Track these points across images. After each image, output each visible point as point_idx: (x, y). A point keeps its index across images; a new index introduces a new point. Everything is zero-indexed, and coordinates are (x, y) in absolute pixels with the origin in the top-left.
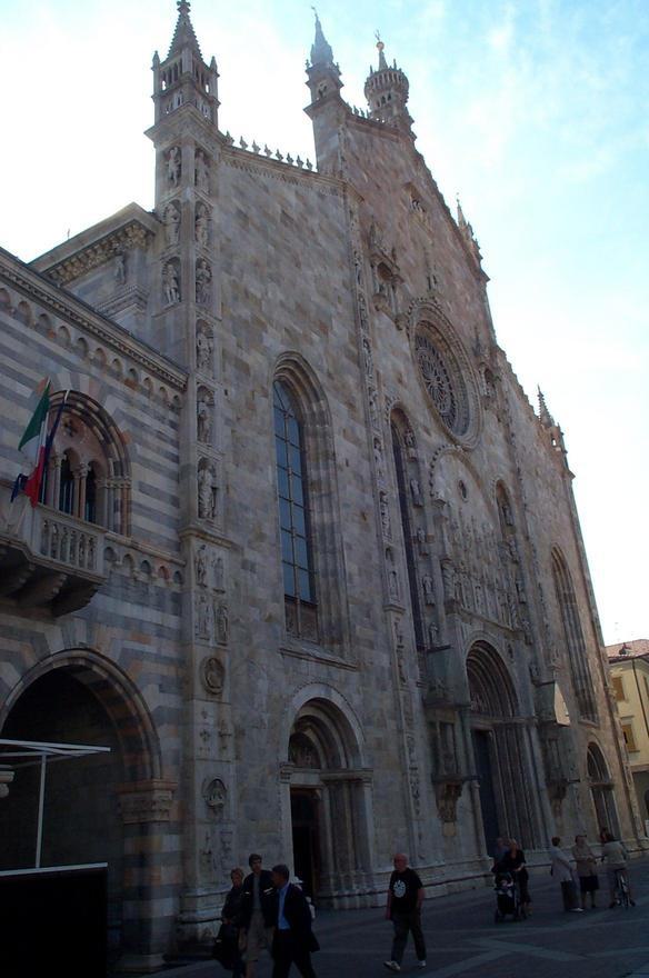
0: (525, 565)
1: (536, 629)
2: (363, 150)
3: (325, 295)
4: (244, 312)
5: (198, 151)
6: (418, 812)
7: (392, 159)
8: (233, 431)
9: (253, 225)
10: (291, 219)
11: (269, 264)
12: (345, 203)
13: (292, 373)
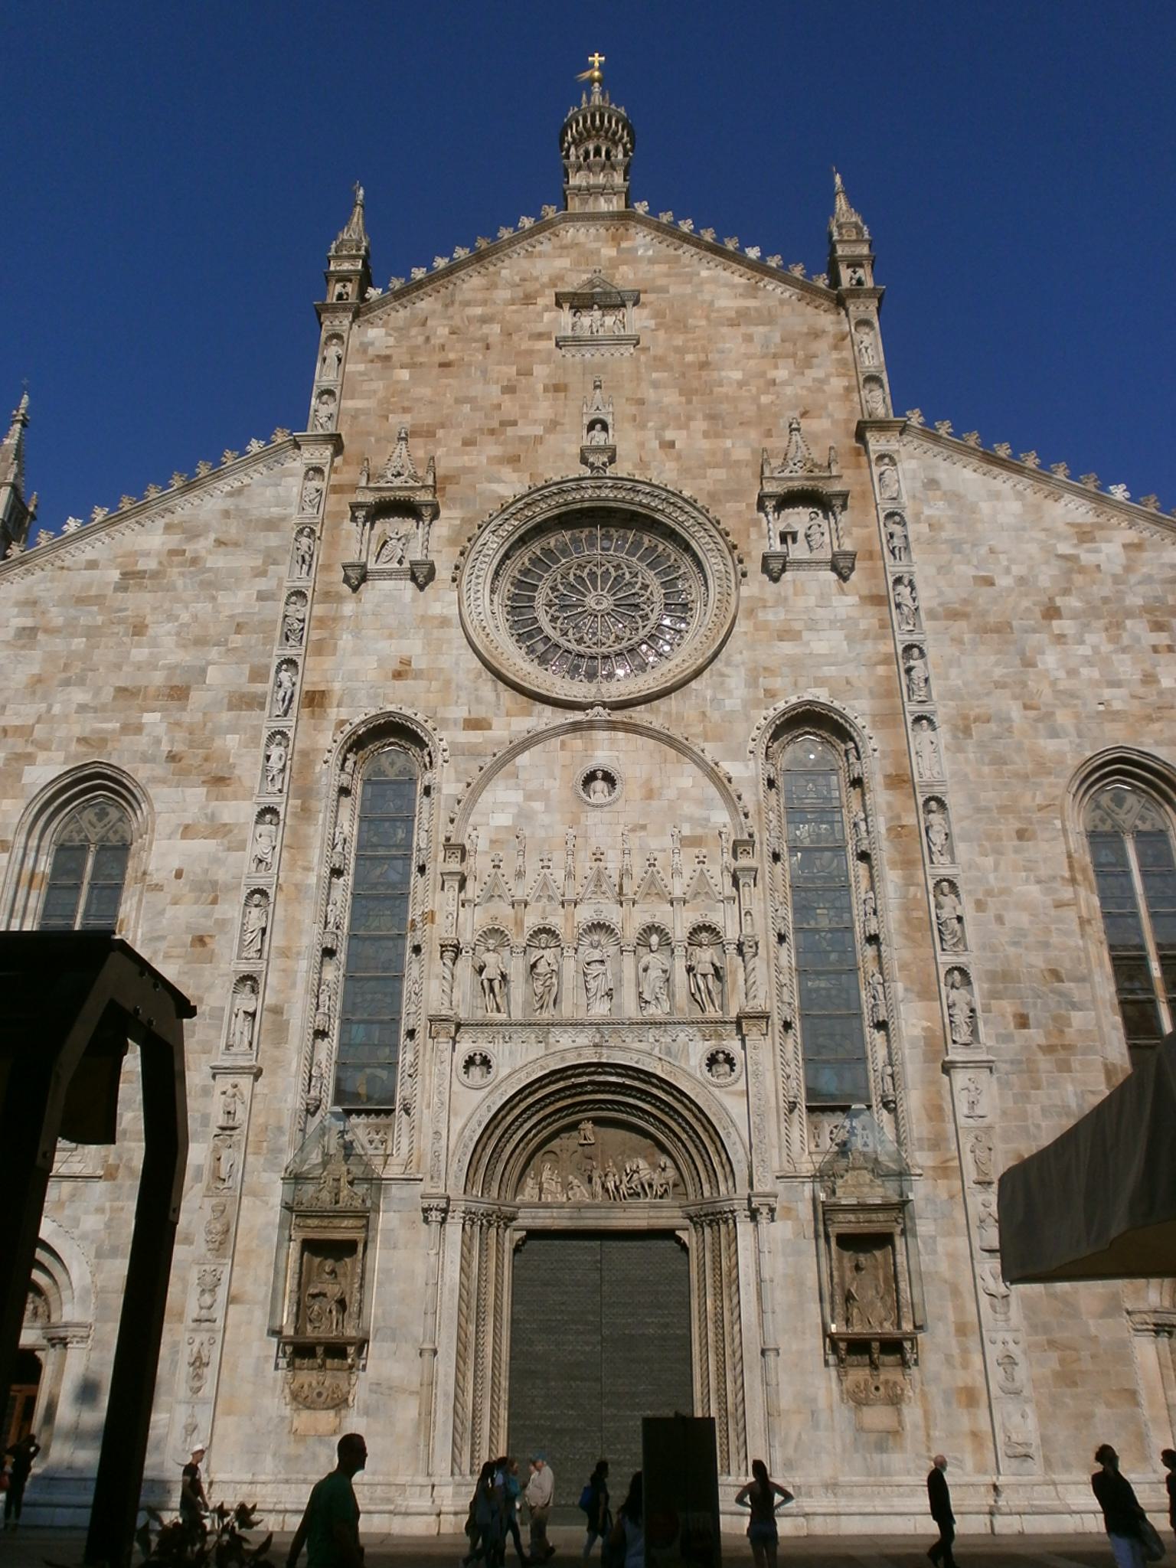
0: (884, 852)
1: (899, 988)
3: (200, 642)
9: (46, 631)
10: (141, 575)
11: (66, 667)
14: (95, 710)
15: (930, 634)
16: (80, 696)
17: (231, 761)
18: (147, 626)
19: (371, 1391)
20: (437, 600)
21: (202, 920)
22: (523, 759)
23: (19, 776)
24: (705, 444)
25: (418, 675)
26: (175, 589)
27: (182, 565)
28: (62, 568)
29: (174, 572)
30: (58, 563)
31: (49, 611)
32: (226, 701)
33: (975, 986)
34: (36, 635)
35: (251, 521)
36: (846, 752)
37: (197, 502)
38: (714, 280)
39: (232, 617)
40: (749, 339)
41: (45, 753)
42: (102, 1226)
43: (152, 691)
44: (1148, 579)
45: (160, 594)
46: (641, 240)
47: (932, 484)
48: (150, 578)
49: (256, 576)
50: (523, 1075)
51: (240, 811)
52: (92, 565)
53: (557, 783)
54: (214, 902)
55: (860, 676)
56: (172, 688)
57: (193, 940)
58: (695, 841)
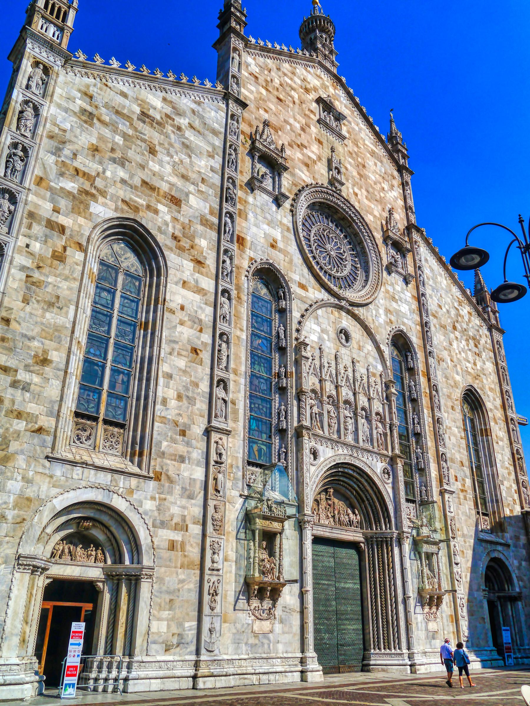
2: (266, 72)
3: (184, 177)
4: (71, 186)
5: (36, 64)
6: (212, 609)
7: (304, 80)
8: (27, 276)
9: (99, 120)
10: (153, 119)
11: (113, 150)
12: (227, 110)
13: (132, 237)
14: (132, 188)
15: (433, 321)
16: (122, 173)
17: (204, 254)
18: (157, 152)
19: (283, 611)
20: (285, 217)
21: (196, 340)
22: (320, 312)
23: (87, 207)
24: (366, 202)
25: (280, 251)
26: (170, 139)
27: (173, 126)
28: (107, 86)
29: (169, 129)
30: (106, 83)
31: (100, 108)
32: (199, 218)
33: (448, 462)
34: (92, 119)
35: (205, 124)
36: (407, 357)
37: (178, 95)
38: (365, 131)
39: (199, 172)
40: (376, 164)
41: (103, 199)
42: (155, 509)
43: (162, 193)
44: (473, 327)
45: (162, 137)
46: (341, 93)
47: (426, 260)
48: (157, 123)
49: (210, 156)
50: (327, 462)
51: (208, 284)
52: (125, 95)
53: (331, 329)
54: (201, 331)
55: (413, 326)
56: (172, 196)
57: (191, 349)
58: (374, 375)
